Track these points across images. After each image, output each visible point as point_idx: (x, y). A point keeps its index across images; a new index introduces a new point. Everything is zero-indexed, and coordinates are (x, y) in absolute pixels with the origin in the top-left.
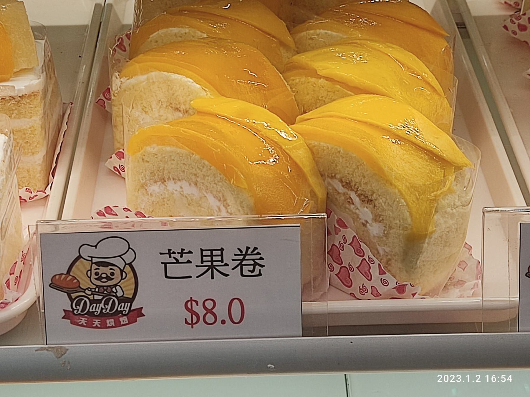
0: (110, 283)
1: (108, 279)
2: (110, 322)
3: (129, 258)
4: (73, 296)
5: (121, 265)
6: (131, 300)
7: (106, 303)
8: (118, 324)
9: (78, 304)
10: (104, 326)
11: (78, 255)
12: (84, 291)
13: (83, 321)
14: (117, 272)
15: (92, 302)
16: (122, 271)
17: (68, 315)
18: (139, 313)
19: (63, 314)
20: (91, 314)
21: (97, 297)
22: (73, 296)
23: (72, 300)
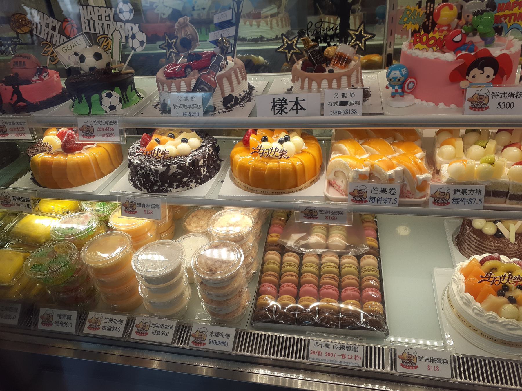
0: (483, 100)
1: (482, 99)
2: (480, 110)
3: (488, 94)
4: (473, 103)
5: (486, 96)
6: (487, 104)
7: (480, 105)
8: (482, 110)
9: (473, 105)
10: (479, 110)
11: (475, 93)
12: (475, 102)
13: (474, 109)
14: (484, 97)
15: (477, 104)
16: (486, 97)
17: (471, 108)
18: (488, 107)
19: (469, 107)
20: (476, 108)
21: (478, 103)
22: (473, 103)
23: (472, 104)
